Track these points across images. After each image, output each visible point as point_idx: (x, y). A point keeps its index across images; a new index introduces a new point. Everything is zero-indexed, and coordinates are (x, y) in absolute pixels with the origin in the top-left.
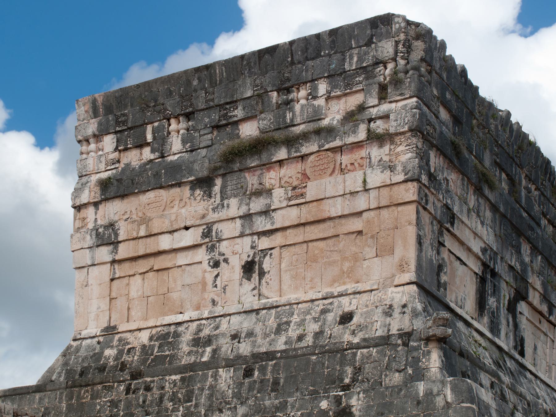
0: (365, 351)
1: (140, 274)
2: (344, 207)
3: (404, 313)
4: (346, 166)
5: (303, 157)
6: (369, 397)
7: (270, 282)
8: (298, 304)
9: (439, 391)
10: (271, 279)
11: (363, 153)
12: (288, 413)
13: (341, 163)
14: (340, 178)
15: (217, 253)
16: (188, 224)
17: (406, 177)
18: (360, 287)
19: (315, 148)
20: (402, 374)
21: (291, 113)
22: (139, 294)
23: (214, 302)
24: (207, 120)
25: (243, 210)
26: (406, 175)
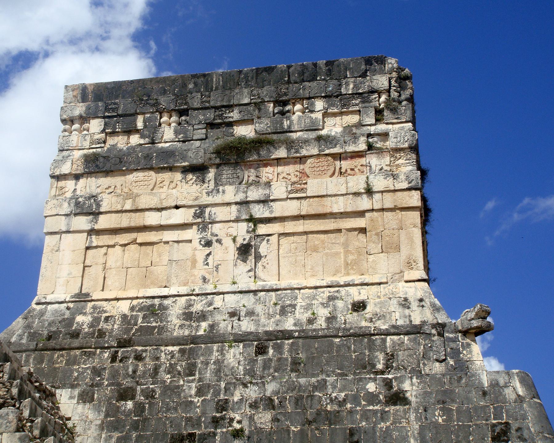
0: (395, 338)
1: (121, 245)
2: (346, 205)
3: (423, 306)
4: (346, 170)
5: (302, 160)
6: (425, 383)
7: (267, 266)
8: (300, 289)
9: (506, 383)
10: (268, 264)
11: (363, 161)
12: (329, 393)
13: (341, 168)
14: (342, 179)
15: (210, 233)
16: (179, 203)
17: (410, 185)
18: (367, 279)
19: (315, 151)
20: (443, 364)
21: (288, 122)
22: (118, 264)
23: (204, 279)
24: (202, 117)
25: (240, 197)
26: (409, 183)
